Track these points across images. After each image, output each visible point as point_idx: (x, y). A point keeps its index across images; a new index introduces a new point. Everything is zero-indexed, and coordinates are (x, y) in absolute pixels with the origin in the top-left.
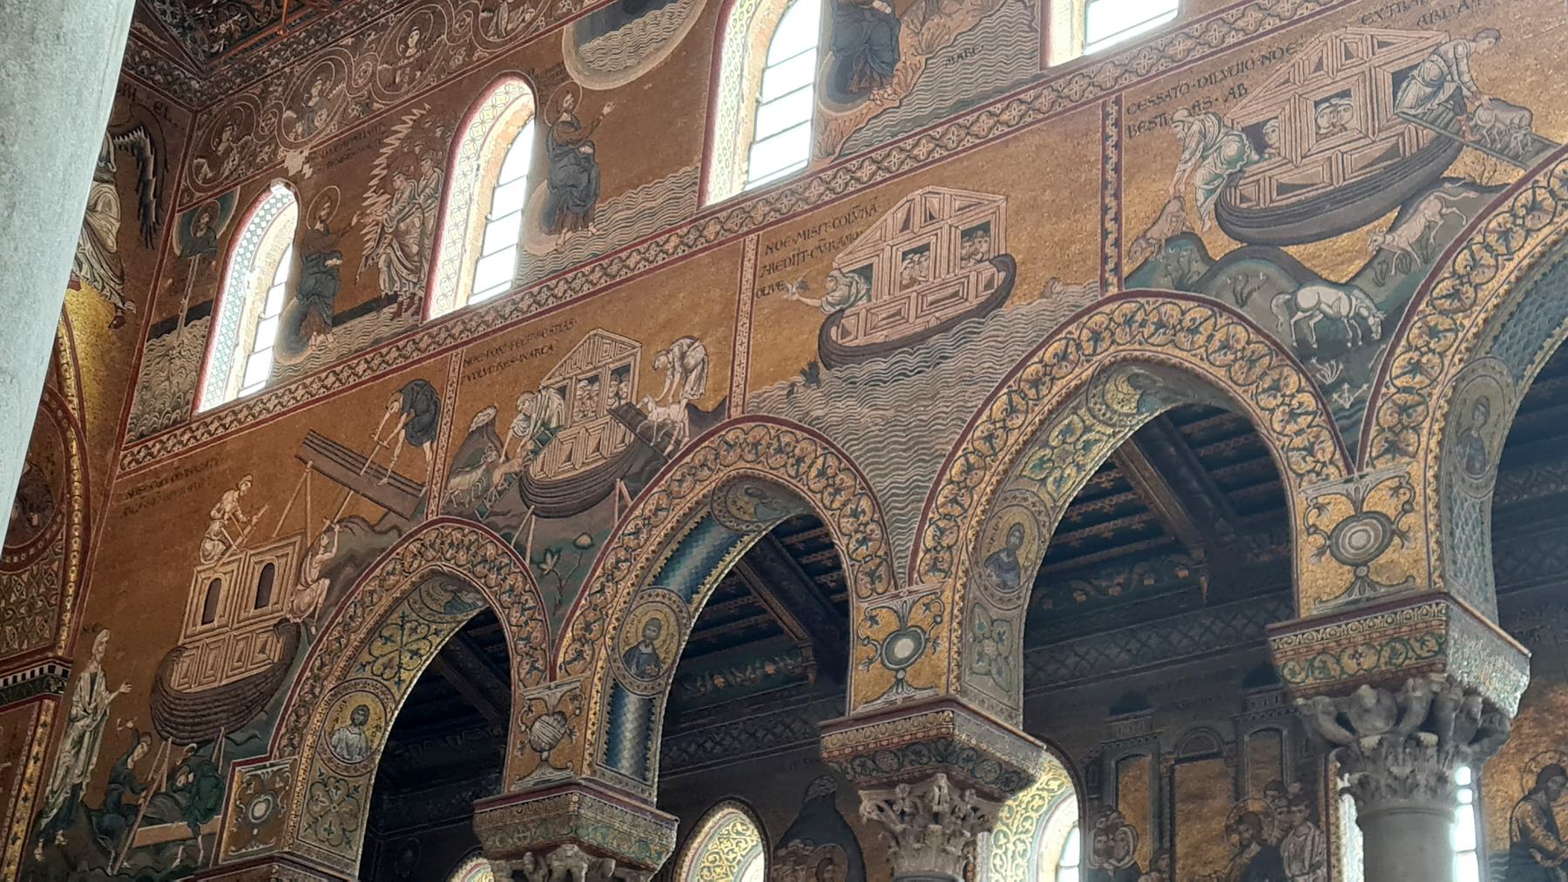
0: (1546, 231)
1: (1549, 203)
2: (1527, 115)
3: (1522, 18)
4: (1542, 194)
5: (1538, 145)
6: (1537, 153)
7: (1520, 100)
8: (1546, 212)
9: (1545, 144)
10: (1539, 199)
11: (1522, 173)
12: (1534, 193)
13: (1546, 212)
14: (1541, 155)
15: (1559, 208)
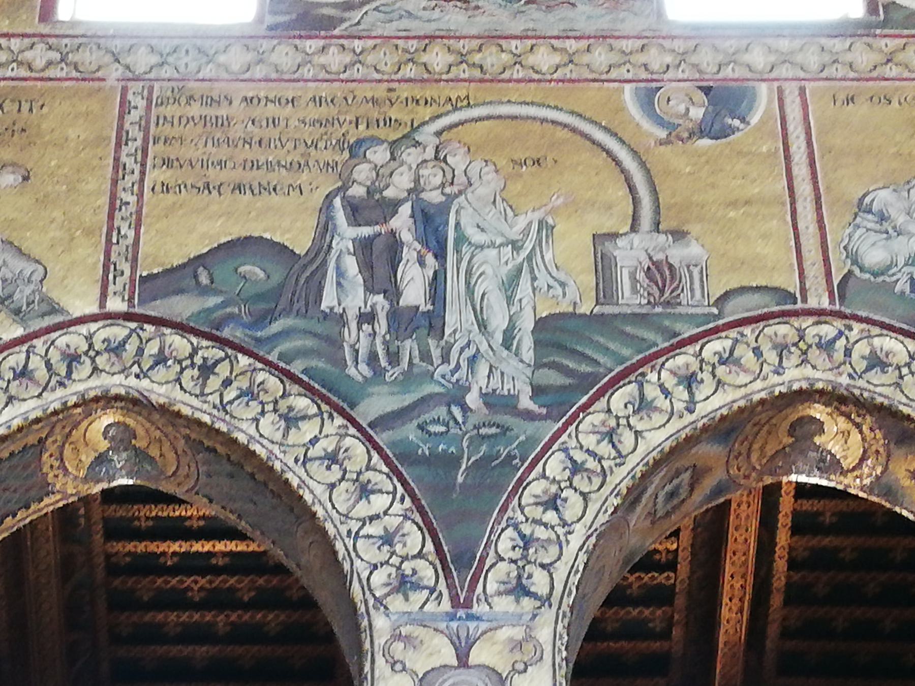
0: (32, 403)
1: (41, 374)
2: (41, 269)
3: (59, 167)
4: (36, 362)
5: (45, 307)
6: (43, 315)
7: (36, 252)
8: (37, 383)
9: (54, 309)
10: (31, 366)
11: (19, 332)
12: (28, 358)
13: (37, 383)
14: (46, 318)
15: (53, 382)
